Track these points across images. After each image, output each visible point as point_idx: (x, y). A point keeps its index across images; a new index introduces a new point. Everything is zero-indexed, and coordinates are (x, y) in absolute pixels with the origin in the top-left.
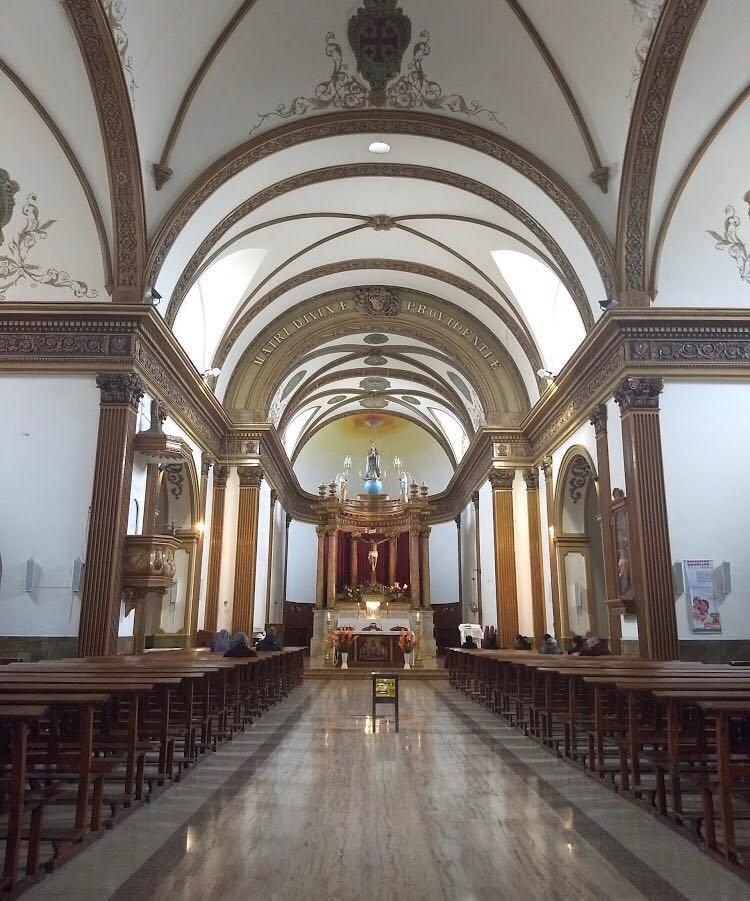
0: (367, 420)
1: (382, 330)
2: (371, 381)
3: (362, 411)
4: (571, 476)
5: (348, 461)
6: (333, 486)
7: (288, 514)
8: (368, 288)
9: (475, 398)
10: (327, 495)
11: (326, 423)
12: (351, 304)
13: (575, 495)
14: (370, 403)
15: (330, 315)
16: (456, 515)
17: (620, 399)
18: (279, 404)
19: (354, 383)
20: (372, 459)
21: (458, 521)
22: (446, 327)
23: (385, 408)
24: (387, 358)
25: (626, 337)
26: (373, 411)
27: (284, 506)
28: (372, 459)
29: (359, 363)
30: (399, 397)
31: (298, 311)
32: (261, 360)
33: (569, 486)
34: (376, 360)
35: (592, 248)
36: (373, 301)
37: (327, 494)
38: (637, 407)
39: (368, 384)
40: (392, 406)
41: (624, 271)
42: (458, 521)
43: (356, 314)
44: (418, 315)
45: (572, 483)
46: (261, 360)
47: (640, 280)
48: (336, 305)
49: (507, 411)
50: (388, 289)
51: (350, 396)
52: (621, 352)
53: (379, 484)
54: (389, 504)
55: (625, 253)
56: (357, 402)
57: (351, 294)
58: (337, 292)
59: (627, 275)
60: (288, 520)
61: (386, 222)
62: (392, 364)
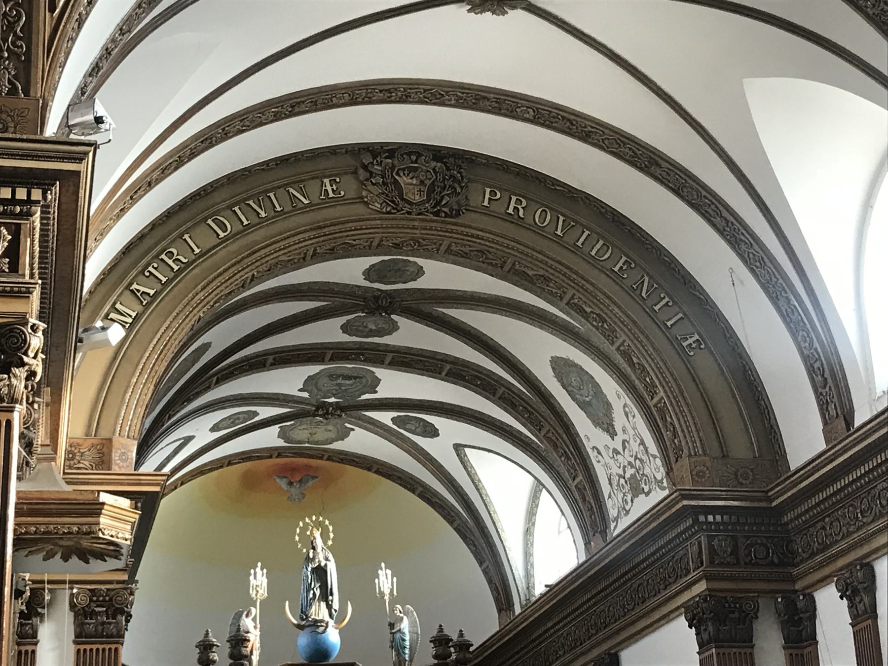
2: (332, 376)
3: (277, 452)
12: (349, 187)
14: (303, 432)
15: (297, 209)
22: (574, 250)
26: (299, 453)
30: (385, 417)
31: (218, 197)
36: (403, 180)
39: (324, 382)
43: (359, 210)
48: (313, 187)
50: (439, 154)
51: (265, 412)
53: (333, 636)
56: (275, 429)
57: (349, 160)
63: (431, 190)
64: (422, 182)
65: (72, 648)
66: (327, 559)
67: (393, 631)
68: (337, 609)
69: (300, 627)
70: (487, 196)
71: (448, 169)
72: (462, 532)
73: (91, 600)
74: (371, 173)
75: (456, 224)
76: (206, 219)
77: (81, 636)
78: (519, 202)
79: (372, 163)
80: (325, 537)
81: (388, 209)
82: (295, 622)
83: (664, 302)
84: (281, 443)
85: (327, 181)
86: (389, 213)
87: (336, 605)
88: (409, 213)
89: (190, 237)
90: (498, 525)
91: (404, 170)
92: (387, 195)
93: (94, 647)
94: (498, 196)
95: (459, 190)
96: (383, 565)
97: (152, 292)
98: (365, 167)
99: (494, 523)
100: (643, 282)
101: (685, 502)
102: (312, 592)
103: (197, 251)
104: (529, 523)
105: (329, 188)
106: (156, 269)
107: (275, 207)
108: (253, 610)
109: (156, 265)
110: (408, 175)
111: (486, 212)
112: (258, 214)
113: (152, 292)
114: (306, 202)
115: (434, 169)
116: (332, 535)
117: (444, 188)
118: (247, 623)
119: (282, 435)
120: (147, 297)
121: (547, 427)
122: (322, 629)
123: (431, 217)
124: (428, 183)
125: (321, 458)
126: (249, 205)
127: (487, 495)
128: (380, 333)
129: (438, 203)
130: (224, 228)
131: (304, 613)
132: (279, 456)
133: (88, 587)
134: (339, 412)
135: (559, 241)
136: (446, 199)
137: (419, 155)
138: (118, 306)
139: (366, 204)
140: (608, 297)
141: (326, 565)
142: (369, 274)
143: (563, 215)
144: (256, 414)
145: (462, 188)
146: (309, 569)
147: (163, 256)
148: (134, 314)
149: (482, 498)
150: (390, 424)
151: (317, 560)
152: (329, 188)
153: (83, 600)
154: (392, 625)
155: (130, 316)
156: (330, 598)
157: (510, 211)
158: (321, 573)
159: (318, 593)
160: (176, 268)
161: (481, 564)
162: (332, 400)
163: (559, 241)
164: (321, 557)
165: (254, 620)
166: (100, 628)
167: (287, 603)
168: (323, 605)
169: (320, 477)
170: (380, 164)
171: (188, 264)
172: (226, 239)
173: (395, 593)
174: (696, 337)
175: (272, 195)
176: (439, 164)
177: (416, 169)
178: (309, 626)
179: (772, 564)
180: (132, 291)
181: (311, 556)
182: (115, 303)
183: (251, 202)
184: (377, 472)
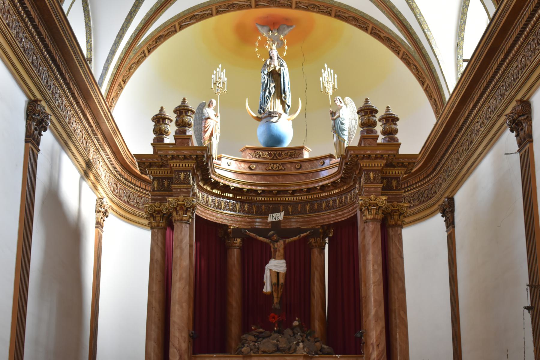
0: (263, 25)
7: (100, 203)
16: (444, 199)
54: (307, 167)
67: (334, 118)
68: (290, 104)
69: (259, 119)
72: (407, 60)
80: (280, 48)
82: (255, 115)
87: (289, 102)
90: (432, 41)
96: (326, 65)
99: (428, 40)
102: (268, 91)
104: (459, 39)
108: (214, 101)
116: (286, 48)
118: (209, 112)
122: (274, 120)
127: (421, 14)
131: (262, 109)
141: (280, 69)
146: (266, 73)
149: (416, 17)
151: (272, 66)
154: (333, 114)
156: (284, 95)
158: (275, 76)
159: (273, 91)
161: (422, 84)
164: (276, 63)
165: (215, 109)
167: (247, 99)
168: (278, 102)
169: (294, 26)
173: (336, 87)
178: (266, 117)
181: (268, 63)
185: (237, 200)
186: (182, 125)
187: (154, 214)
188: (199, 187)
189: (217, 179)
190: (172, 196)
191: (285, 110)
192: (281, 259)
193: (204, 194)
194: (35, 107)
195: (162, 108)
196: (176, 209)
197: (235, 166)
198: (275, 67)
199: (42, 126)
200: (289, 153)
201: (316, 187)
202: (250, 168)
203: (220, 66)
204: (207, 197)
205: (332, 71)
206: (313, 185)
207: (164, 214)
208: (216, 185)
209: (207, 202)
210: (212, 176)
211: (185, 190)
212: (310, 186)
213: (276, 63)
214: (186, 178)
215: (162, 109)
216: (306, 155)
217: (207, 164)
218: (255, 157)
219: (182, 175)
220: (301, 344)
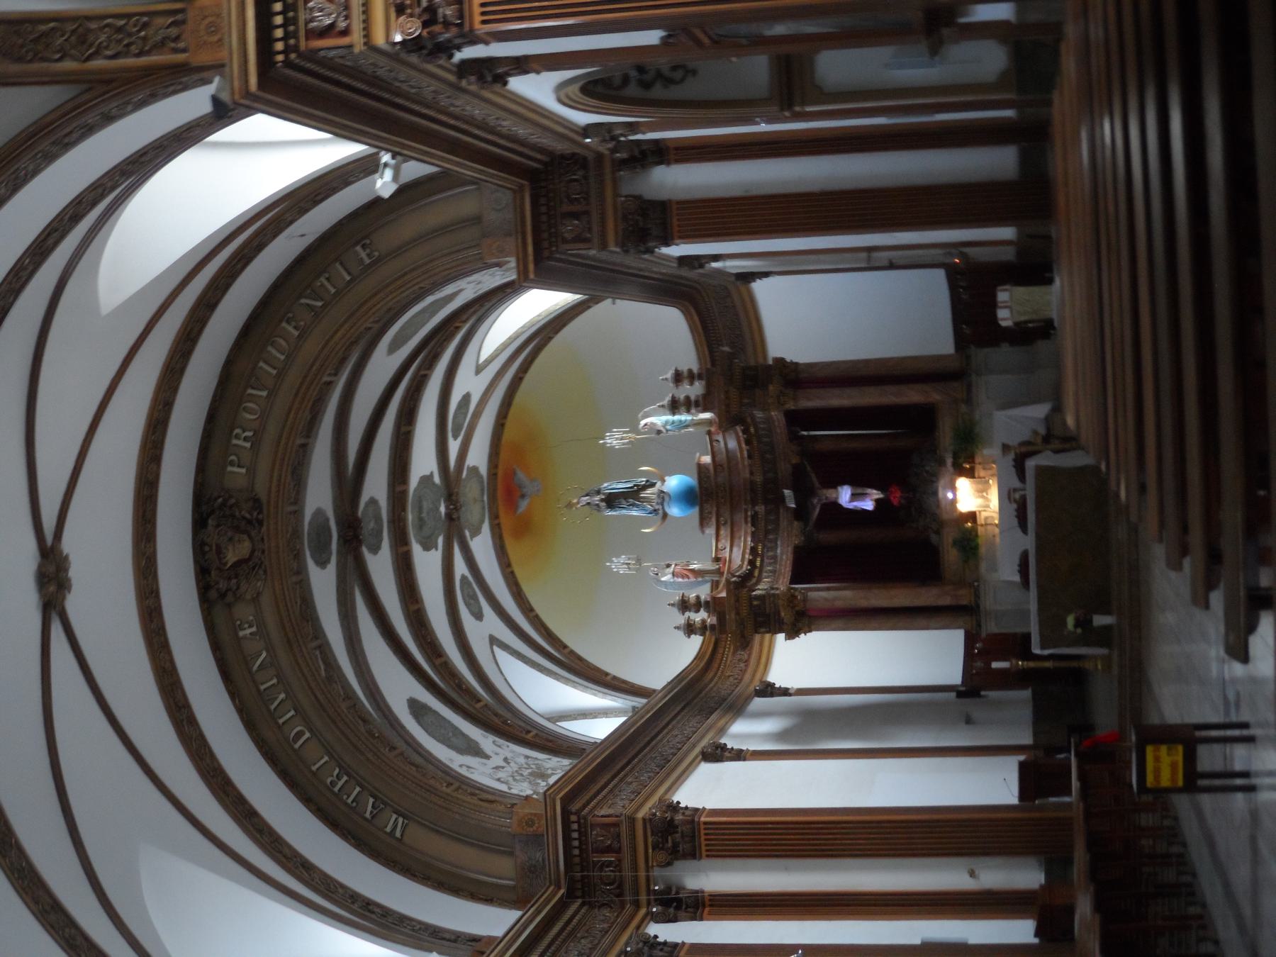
1: (297, 534)
2: (421, 523)
4: (633, 90)
5: (619, 564)
6: (684, 605)
8: (202, 571)
9: (449, 290)
10: (711, 620)
11: (527, 609)
12: (244, 611)
13: (678, 75)
17: (446, 49)
18: (497, 761)
19: (427, 565)
20: (612, 501)
21: (747, 277)
22: (281, 375)
23: (483, 470)
24: (364, 498)
25: (295, 49)
27: (737, 708)
28: (612, 501)
29: (380, 566)
30: (454, 446)
32: (393, 822)
33: (658, 92)
34: (368, 526)
35: (89, 130)
36: (231, 557)
37: (699, 617)
38: (461, 17)
40: (478, 456)
41: (144, 60)
42: (747, 277)
43: (266, 599)
44: (256, 442)
45: (646, 85)
46: (393, 822)
47: (160, 21)
49: (477, 220)
50: (199, 523)
51: (460, 568)
52: (332, 54)
53: (674, 483)
55: (98, 63)
58: (216, 647)
59: (148, 53)
60: (769, 690)
61: (51, 569)
62: (376, 485)
63: (237, 529)
64: (231, 539)
65: (705, 862)
66: (598, 492)
70: (236, 469)
71: (213, 512)
73: (662, 849)
74: (227, 590)
75: (269, 502)
76: (295, 750)
77: (693, 855)
78: (237, 437)
79: (218, 589)
81: (261, 572)
83: (326, 283)
84: (486, 528)
85: (241, 634)
86: (265, 572)
88: (263, 552)
89: (315, 764)
91: (220, 559)
92: (248, 573)
93: (703, 843)
94: (233, 458)
95: (233, 501)
97: (371, 800)
98: (223, 596)
100: (308, 305)
101: (532, 276)
103: (326, 758)
105: (248, 631)
106: (349, 797)
107: (273, 685)
109: (345, 797)
110: (225, 553)
111: (252, 471)
112: (282, 701)
113: (371, 800)
114: (264, 654)
115: (218, 526)
117: (233, 516)
119: (476, 531)
120: (377, 804)
121: (457, 325)
123: (264, 529)
124: (230, 534)
125: (495, 474)
126: (275, 709)
128: (378, 508)
129: (249, 522)
130: (300, 734)
132: (497, 517)
133: (650, 851)
134: (454, 498)
135: (273, 393)
136: (243, 513)
137: (203, 544)
138: (388, 829)
139: (259, 594)
140: (327, 343)
142: (322, 563)
143: (245, 389)
144: (464, 578)
145: (231, 497)
147: (336, 789)
148: (394, 816)
150: (460, 439)
152: (248, 631)
153: (662, 856)
155: (396, 819)
157: (248, 445)
160: (345, 778)
162: (443, 509)
163: (273, 393)
166: (687, 839)
170: (217, 583)
171: (341, 767)
172: (311, 731)
174: (358, 248)
175: (262, 687)
176: (210, 521)
177: (217, 545)
179: (585, 178)
180: (373, 817)
182: (385, 832)
183: (273, 707)
184: (505, 417)
185: (766, 536)
186: (698, 605)
187: (796, 629)
188: (758, 582)
189: (746, 563)
190: (779, 613)
191: (653, 485)
192: (837, 491)
193: (763, 577)
194: (710, 754)
195: (675, 628)
196: (793, 608)
197: (725, 543)
198: (602, 500)
199: (723, 747)
200: (705, 479)
201: (748, 451)
202: (725, 523)
203: (608, 564)
204: (766, 572)
205: (608, 434)
206: (745, 453)
207: (795, 619)
208: (752, 563)
209: (771, 571)
210: (744, 569)
211: (772, 599)
212: (746, 455)
213: (597, 498)
214: (757, 597)
215: (677, 628)
216: (707, 459)
217: (739, 576)
218: (711, 518)
219: (755, 603)
220: (928, 468)
